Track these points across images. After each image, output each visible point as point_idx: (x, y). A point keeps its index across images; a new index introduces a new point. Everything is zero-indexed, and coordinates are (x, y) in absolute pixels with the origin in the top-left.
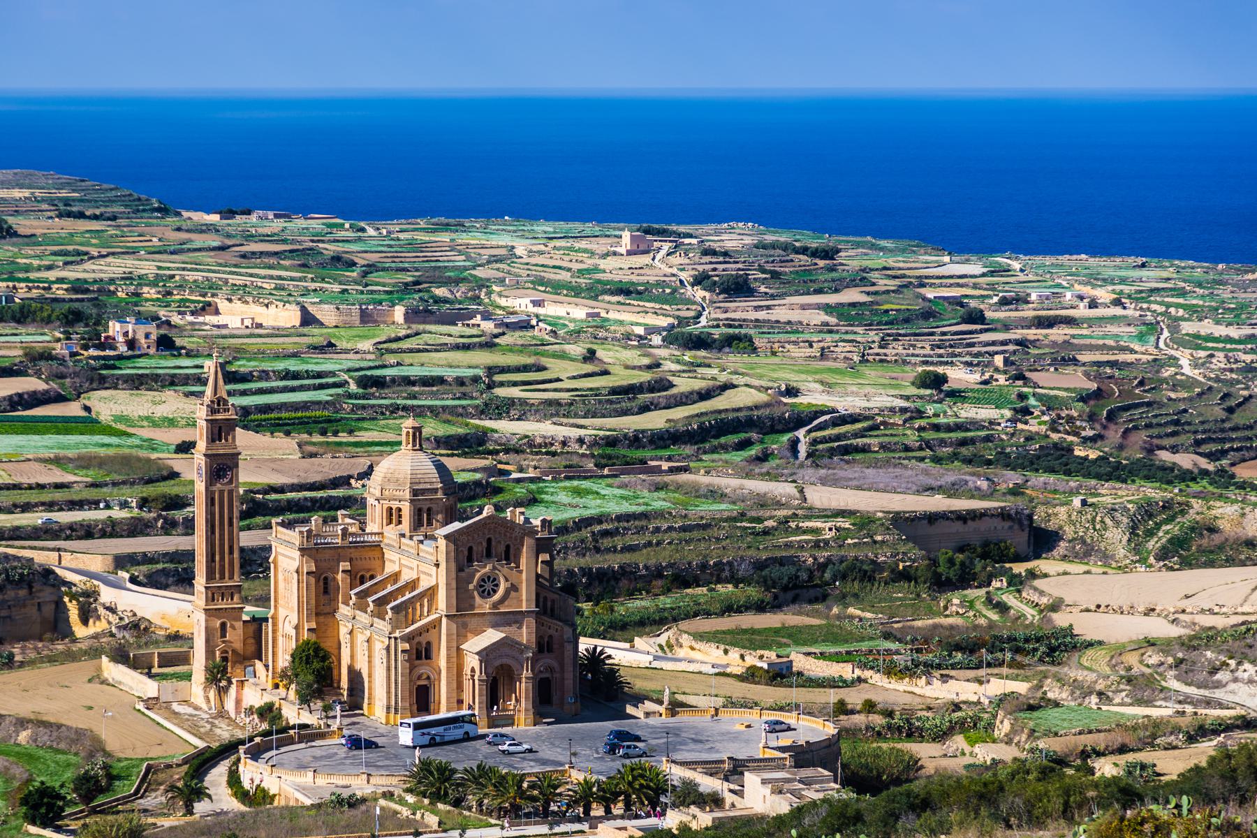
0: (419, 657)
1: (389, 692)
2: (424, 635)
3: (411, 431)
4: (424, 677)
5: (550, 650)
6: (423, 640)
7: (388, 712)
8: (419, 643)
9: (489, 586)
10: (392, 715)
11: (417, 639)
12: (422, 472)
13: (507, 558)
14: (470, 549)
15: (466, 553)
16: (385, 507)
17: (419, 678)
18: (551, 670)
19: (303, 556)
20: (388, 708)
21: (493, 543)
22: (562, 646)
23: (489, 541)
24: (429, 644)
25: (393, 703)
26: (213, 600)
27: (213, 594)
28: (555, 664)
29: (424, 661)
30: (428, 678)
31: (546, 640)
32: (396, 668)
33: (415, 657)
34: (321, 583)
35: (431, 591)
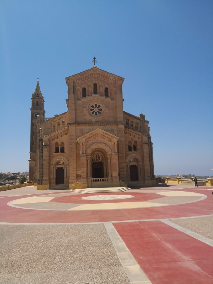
0: (57, 151)
4: (61, 162)
5: (135, 149)
6: (59, 141)
9: (96, 110)
13: (107, 95)
14: (84, 90)
15: (81, 90)
17: (58, 163)
18: (136, 160)
21: (98, 86)
22: (142, 146)
23: (95, 85)
24: (63, 143)
28: (139, 157)
29: (60, 153)
31: (133, 143)
33: (54, 150)
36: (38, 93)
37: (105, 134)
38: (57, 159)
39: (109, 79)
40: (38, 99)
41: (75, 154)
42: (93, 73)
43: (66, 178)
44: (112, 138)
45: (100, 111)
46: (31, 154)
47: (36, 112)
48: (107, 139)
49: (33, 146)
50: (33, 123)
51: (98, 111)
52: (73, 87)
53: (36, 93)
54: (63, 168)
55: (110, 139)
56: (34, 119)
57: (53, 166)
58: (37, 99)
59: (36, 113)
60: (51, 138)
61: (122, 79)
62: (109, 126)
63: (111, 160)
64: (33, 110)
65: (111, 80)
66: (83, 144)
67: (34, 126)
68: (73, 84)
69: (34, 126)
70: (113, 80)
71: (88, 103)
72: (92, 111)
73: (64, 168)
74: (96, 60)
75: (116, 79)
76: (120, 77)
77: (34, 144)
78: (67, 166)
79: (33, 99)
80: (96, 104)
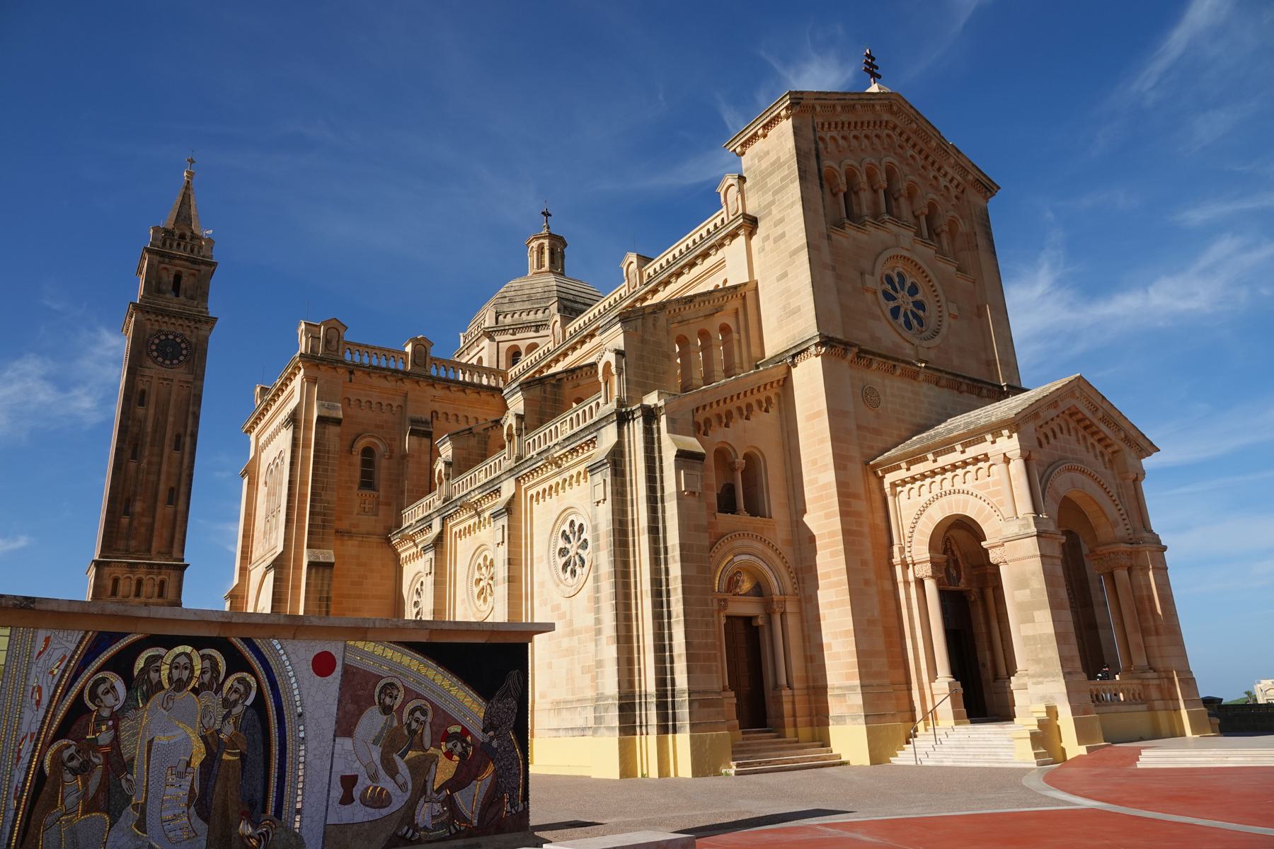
0: (727, 503)
1: (625, 639)
2: (739, 424)
3: (546, 242)
7: (628, 726)
8: (723, 456)
9: (904, 300)
10: (647, 743)
11: (719, 435)
12: (579, 289)
16: (504, 347)
19: (310, 380)
20: (627, 707)
21: (903, 186)
25: (648, 682)
26: (114, 593)
27: (116, 581)
29: (743, 518)
30: (759, 590)
32: (655, 530)
34: (357, 459)
35: (735, 303)
36: (189, 234)
37: (1103, 420)
38: (736, 559)
39: (939, 169)
40: (187, 259)
41: (866, 529)
42: (886, 119)
43: (789, 686)
44: (1122, 445)
45: (921, 313)
46: (107, 570)
47: (164, 328)
48: (1099, 447)
49: (125, 521)
50: (141, 386)
51: (911, 311)
52: (814, 152)
53: (177, 232)
54: (756, 617)
55: (1110, 450)
56: (149, 363)
57: (720, 600)
58: (180, 258)
59: (166, 335)
60: (701, 417)
61: (988, 188)
62: (974, 396)
63: (1130, 570)
64: (153, 317)
65: (949, 177)
66: (1032, 454)
67: (142, 403)
68: (812, 137)
69: (142, 403)
70: (955, 182)
71: (880, 254)
72: (892, 304)
73: (760, 622)
74: (877, 68)
75: (970, 177)
76: (985, 176)
77: (127, 513)
78: (790, 608)
79: (156, 258)
80: (901, 270)
